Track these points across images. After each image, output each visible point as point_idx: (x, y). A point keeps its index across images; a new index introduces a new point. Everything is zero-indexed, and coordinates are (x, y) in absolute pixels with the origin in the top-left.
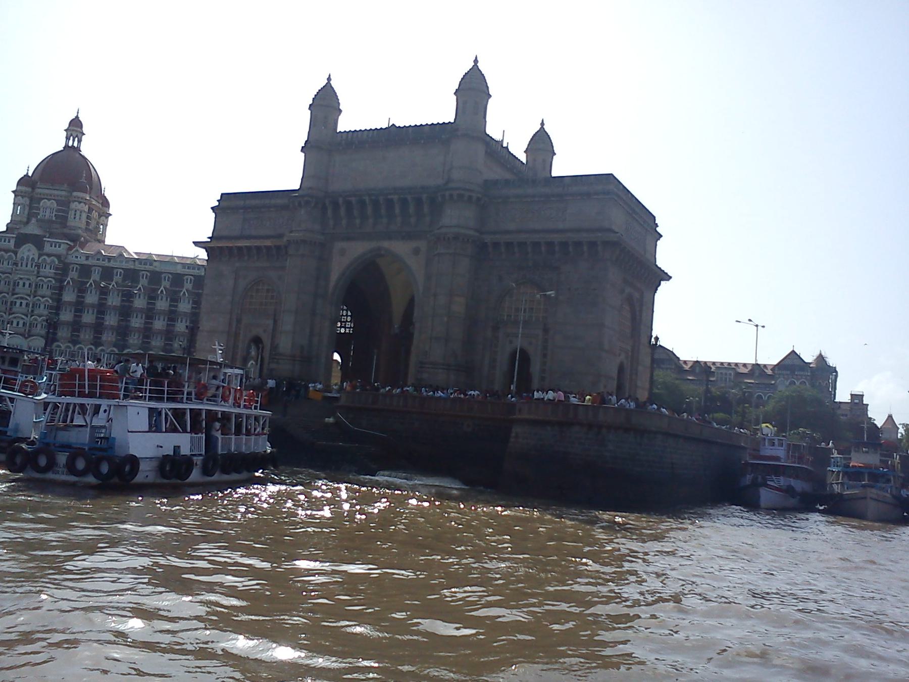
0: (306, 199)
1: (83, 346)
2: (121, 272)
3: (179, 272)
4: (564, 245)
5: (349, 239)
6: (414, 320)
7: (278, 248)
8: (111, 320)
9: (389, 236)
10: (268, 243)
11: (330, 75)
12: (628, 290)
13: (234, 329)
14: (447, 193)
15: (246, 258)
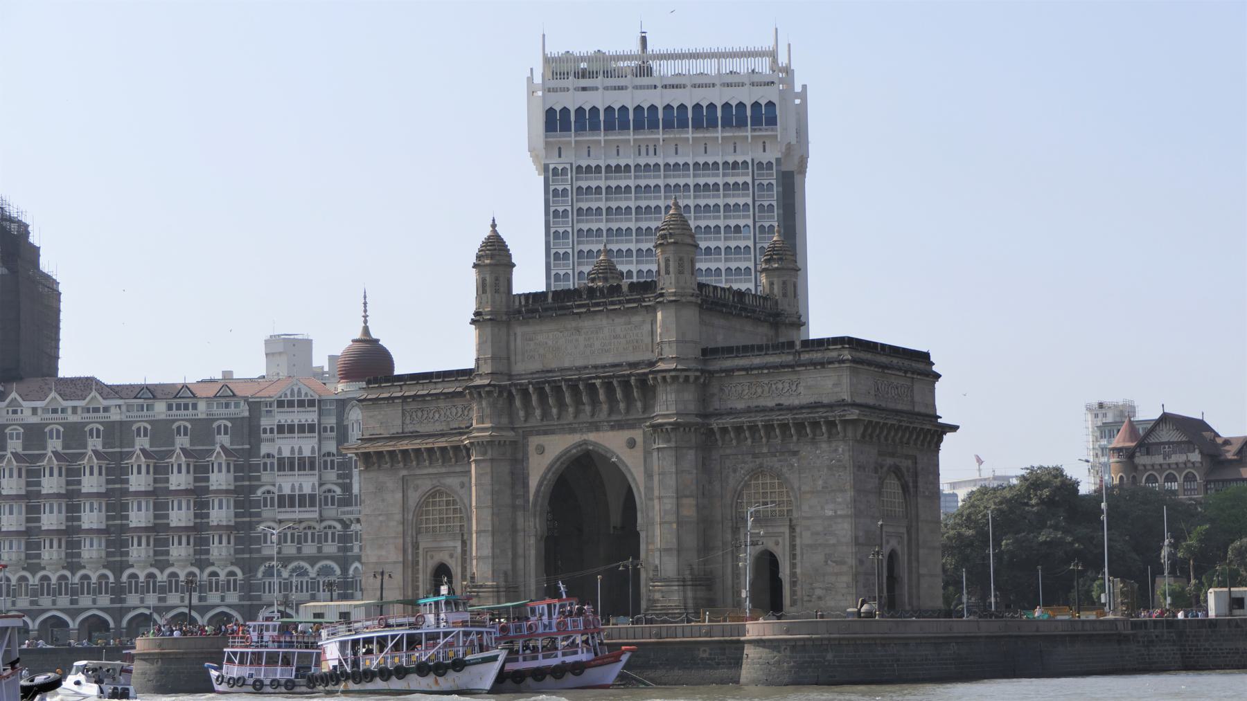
0: (487, 389)
1: (49, 574)
2: (98, 430)
3: (204, 416)
4: (800, 426)
5: (546, 433)
6: (638, 529)
7: (456, 449)
8: (91, 518)
9: (595, 427)
10: (442, 442)
11: (494, 220)
12: (889, 461)
13: (410, 558)
14: (659, 376)
15: (414, 463)
